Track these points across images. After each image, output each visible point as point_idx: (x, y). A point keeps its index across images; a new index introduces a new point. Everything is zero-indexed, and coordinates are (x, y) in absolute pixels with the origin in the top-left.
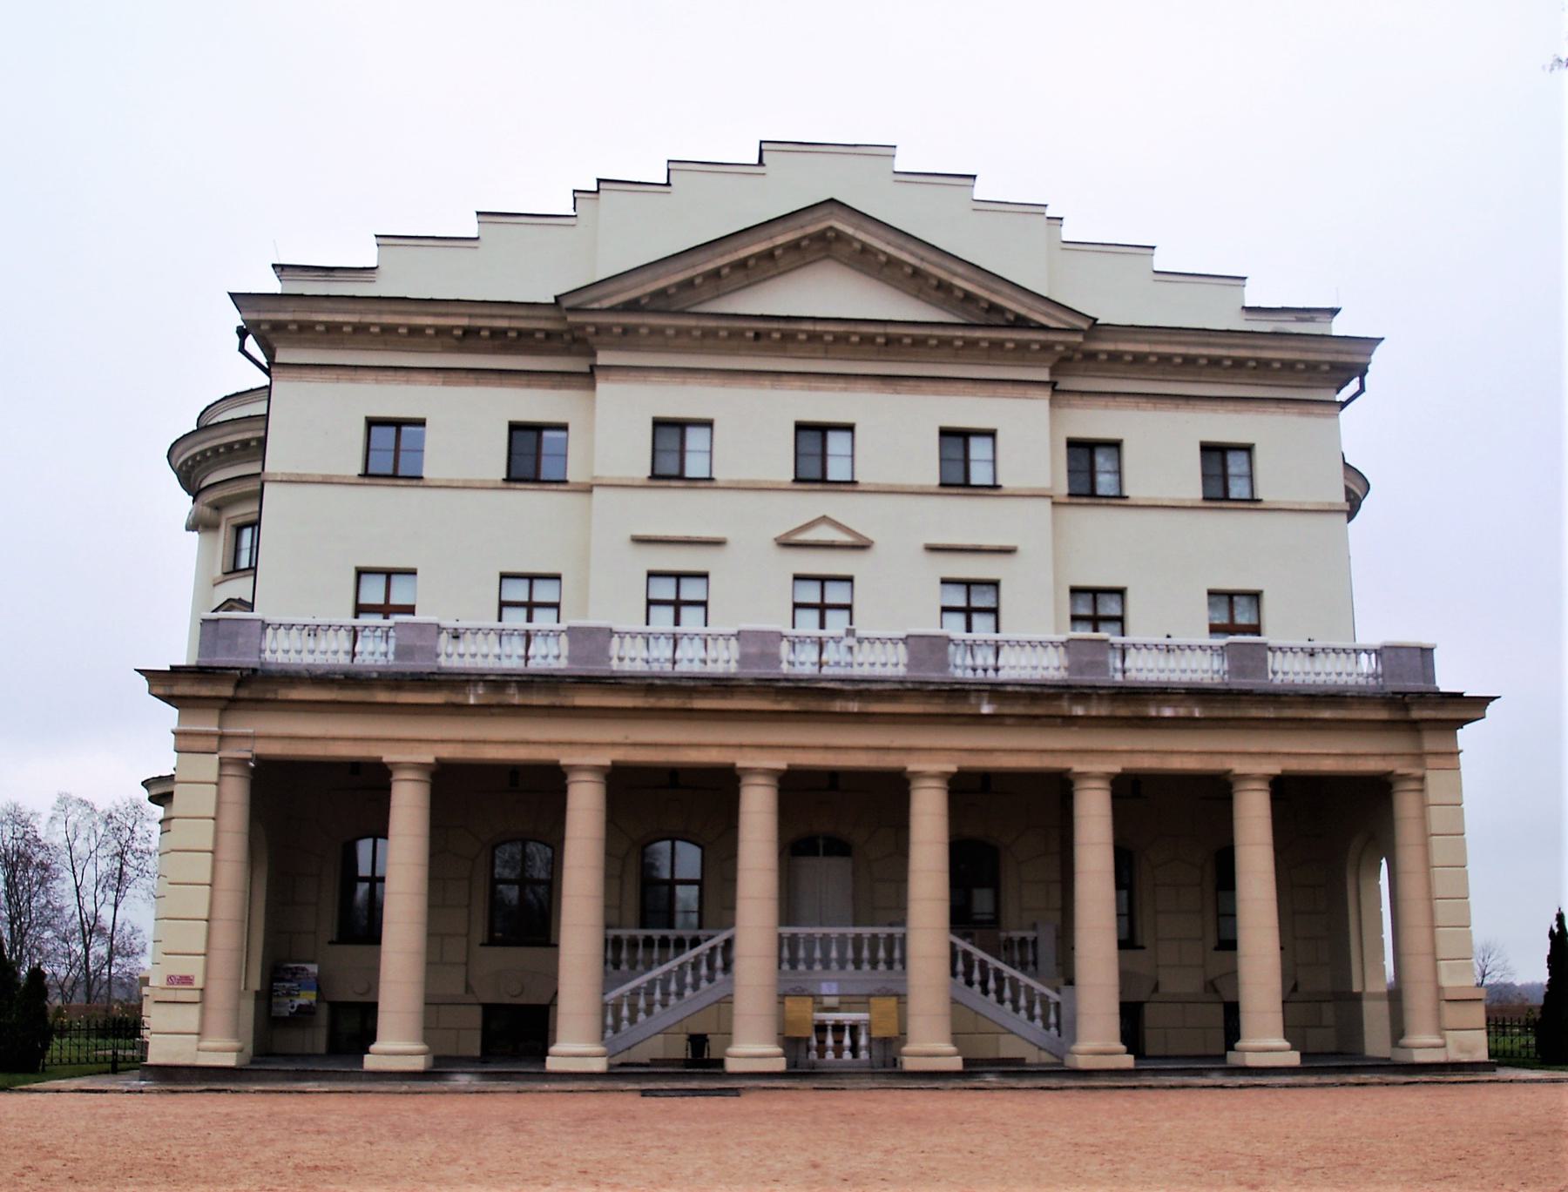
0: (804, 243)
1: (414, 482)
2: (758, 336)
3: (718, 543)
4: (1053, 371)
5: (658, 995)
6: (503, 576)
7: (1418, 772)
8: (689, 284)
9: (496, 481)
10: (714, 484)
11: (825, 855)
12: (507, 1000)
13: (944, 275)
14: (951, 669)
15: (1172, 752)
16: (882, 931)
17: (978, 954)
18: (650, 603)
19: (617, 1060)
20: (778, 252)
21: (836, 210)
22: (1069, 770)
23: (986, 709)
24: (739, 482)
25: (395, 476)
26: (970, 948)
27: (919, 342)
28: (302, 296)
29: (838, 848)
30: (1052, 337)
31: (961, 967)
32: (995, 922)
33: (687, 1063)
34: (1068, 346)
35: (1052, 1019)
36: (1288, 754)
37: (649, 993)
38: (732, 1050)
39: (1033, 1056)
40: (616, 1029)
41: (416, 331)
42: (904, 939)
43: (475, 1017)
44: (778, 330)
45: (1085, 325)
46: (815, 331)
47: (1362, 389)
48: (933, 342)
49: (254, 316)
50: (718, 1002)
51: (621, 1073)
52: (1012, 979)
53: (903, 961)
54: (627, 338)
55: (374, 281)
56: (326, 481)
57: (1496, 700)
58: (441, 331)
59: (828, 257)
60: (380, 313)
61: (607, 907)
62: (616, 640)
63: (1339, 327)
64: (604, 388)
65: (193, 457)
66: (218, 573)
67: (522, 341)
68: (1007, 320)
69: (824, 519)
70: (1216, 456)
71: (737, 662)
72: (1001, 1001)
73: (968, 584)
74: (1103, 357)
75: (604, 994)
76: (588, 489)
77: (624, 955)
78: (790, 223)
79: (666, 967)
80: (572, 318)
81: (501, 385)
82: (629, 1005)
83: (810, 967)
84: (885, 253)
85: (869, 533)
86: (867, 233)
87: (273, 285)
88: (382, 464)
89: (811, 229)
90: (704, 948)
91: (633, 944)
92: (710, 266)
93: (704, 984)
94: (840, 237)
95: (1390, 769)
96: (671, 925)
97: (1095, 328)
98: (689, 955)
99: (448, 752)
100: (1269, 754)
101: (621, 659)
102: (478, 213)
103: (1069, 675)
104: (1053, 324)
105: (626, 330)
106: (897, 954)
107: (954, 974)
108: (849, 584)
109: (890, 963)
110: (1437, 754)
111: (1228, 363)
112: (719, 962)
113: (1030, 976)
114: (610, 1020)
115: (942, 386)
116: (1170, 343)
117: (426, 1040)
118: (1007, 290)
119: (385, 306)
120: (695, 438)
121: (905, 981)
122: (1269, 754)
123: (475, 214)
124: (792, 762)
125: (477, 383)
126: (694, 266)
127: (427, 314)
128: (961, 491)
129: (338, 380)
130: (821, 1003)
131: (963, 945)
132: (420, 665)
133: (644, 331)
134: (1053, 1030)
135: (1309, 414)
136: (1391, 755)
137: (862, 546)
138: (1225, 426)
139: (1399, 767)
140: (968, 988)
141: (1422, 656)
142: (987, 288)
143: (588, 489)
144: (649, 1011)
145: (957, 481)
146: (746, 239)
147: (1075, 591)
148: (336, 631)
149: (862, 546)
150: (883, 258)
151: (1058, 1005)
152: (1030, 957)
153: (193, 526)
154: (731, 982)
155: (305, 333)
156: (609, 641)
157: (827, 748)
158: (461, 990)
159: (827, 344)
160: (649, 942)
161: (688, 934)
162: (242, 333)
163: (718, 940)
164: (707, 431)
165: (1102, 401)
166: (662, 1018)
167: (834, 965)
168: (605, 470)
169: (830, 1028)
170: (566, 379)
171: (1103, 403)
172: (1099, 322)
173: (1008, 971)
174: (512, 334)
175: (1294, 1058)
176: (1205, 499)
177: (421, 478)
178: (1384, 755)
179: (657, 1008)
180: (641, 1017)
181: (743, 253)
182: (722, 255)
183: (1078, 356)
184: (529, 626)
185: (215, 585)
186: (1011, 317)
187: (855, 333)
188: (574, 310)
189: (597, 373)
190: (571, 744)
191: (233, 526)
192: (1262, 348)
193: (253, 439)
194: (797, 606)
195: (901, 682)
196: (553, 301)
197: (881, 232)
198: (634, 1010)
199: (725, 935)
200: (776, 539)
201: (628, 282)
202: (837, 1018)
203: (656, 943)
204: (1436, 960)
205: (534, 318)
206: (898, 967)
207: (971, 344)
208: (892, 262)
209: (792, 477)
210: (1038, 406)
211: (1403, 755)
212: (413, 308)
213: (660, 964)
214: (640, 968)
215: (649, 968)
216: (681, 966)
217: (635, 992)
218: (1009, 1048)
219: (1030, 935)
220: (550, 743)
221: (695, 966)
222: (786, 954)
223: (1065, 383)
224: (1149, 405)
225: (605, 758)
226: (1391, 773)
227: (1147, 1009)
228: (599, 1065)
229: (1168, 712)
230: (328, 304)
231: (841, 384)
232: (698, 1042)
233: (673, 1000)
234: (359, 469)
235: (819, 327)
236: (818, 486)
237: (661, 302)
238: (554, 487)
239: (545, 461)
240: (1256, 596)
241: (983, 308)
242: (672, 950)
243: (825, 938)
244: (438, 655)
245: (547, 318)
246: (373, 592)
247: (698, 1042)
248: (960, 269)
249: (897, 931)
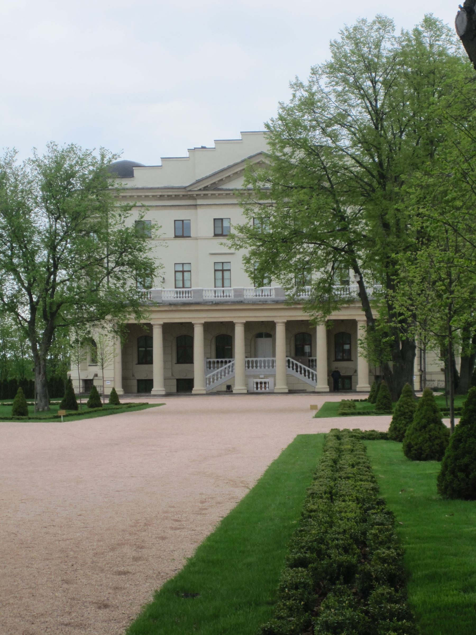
6: (175, 264)
8: (222, 180)
17: (299, 364)
33: (227, 392)
37: (217, 375)
40: (209, 384)
43: (175, 382)
54: (206, 196)
58: (153, 196)
61: (205, 353)
64: (200, 211)
67: (177, 197)
77: (212, 366)
80: (189, 193)
90: (231, 364)
91: (214, 362)
92: (227, 175)
94: (264, 163)
98: (228, 365)
114: (208, 382)
117: (164, 387)
131: (295, 362)
143: (196, 239)
144: (217, 379)
158: (171, 375)
160: (218, 362)
167: (263, 367)
173: (307, 368)
180: (215, 381)
181: (236, 171)
188: (190, 191)
190: (194, 318)
201: (204, 182)
213: (221, 367)
214: (216, 369)
215: (218, 368)
216: (226, 368)
217: (214, 375)
222: (247, 365)
225: (203, 321)
227: (353, 377)
228: (204, 392)
233: (223, 377)
237: (214, 187)
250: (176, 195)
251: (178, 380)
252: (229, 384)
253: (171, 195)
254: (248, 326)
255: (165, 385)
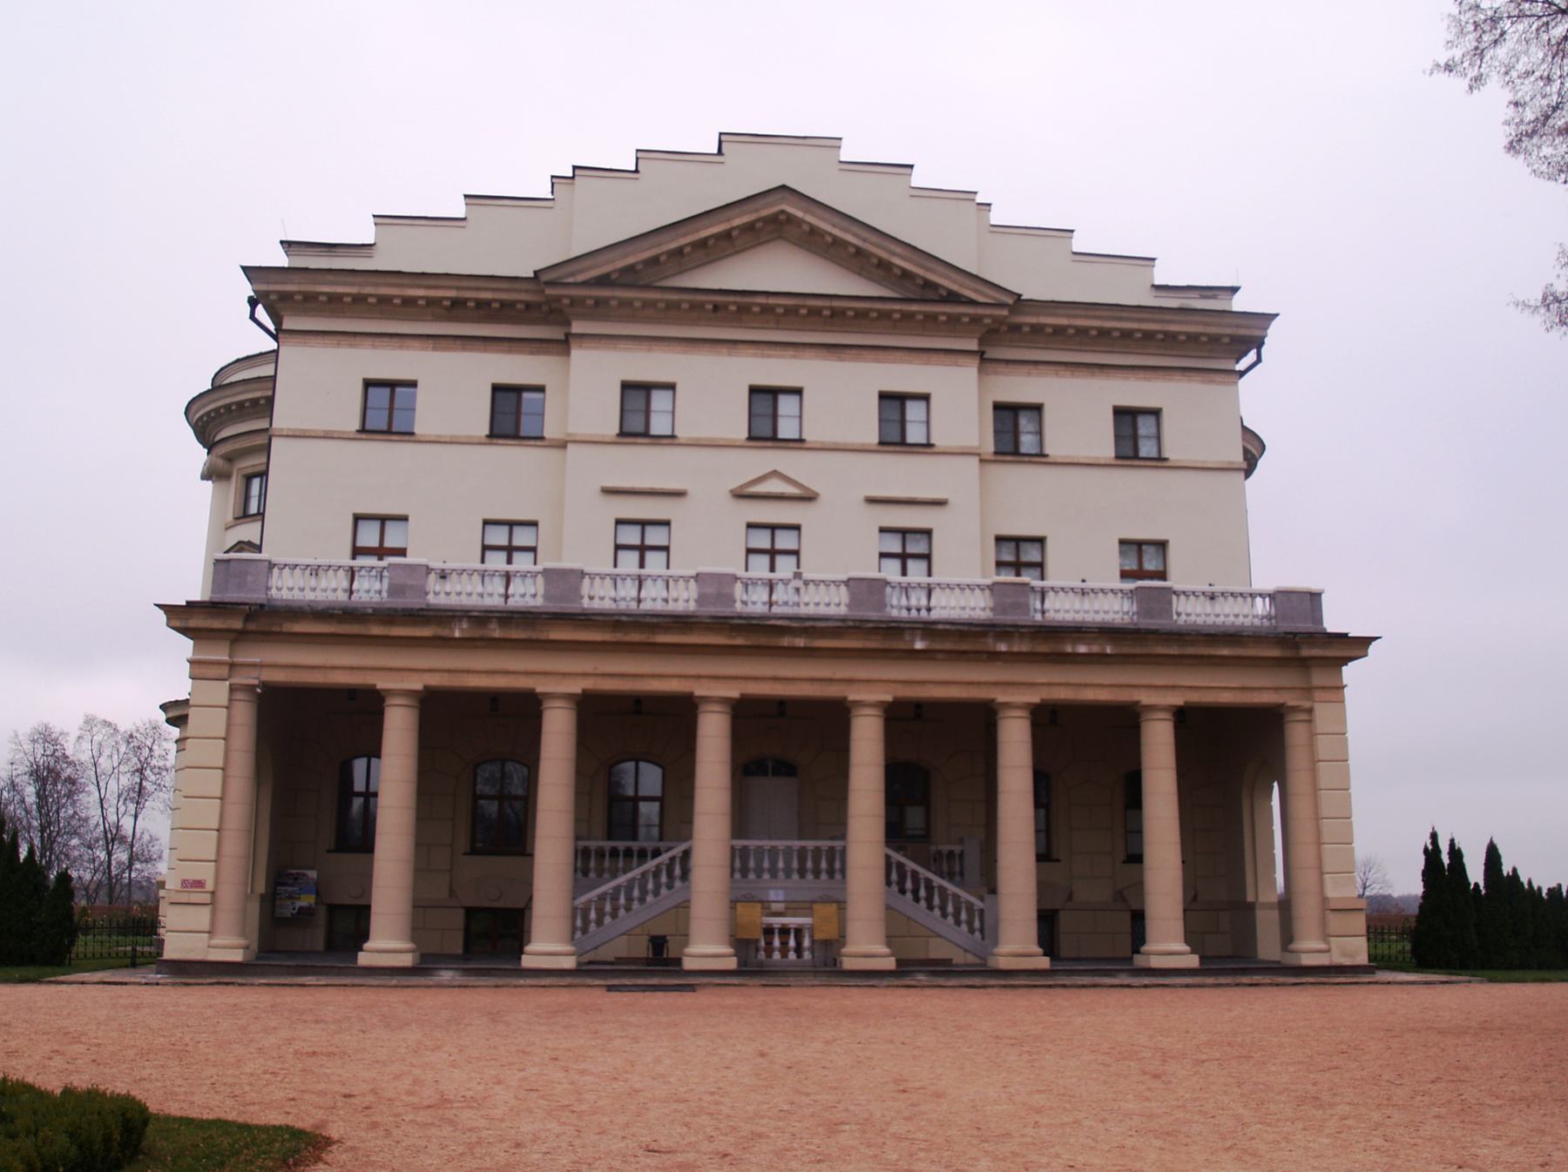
0: (759, 225)
1: (407, 438)
2: (716, 308)
3: (680, 494)
4: (981, 341)
5: (622, 901)
6: (486, 523)
7: (1306, 704)
8: (655, 261)
9: (480, 437)
10: (676, 441)
11: (773, 775)
12: (487, 904)
13: (884, 255)
14: (888, 609)
15: (1086, 685)
16: (824, 844)
17: (911, 865)
18: (618, 547)
19: (586, 958)
20: (735, 233)
21: (787, 195)
22: (993, 700)
23: (919, 645)
24: (698, 439)
25: (389, 432)
26: (903, 860)
27: (861, 315)
28: (306, 269)
29: (786, 769)
30: (980, 311)
31: (894, 876)
32: (926, 836)
33: (647, 961)
34: (994, 319)
35: (977, 924)
36: (1190, 687)
37: (615, 898)
38: (691, 950)
39: (959, 957)
40: (585, 930)
41: (409, 302)
42: (844, 851)
43: (458, 919)
44: (734, 303)
45: (1010, 301)
46: (767, 304)
47: (1259, 360)
48: (874, 315)
49: (263, 287)
50: (676, 907)
51: (590, 970)
52: (940, 887)
53: (843, 871)
54: (599, 309)
55: (372, 257)
56: (327, 436)
57: (1378, 640)
58: (431, 302)
59: (780, 237)
60: (377, 285)
61: (577, 821)
62: (587, 581)
63: (1239, 304)
64: (580, 356)
65: (208, 414)
66: (230, 518)
68: (941, 295)
69: (775, 474)
70: (1128, 419)
71: (696, 601)
72: (930, 907)
73: (904, 533)
74: (1026, 329)
75: (574, 899)
76: (562, 445)
77: (592, 864)
78: (746, 207)
79: (630, 875)
80: (549, 291)
81: (485, 351)
82: (596, 909)
83: (759, 876)
84: (831, 234)
85: (815, 487)
86: (815, 215)
87: (281, 260)
88: (378, 420)
89: (765, 213)
90: (664, 858)
91: (601, 854)
92: (674, 245)
93: (664, 891)
94: (791, 219)
95: (1282, 701)
96: (635, 837)
97: (1019, 303)
98: (651, 864)
99: (435, 680)
100: (1174, 687)
101: (591, 598)
102: (466, 196)
103: (994, 615)
104: (981, 299)
105: (598, 302)
106: (837, 865)
107: (888, 883)
108: (796, 532)
109: (831, 873)
110: (1323, 688)
111: (1139, 335)
112: (677, 871)
113: (957, 885)
114: (579, 923)
115: (881, 355)
116: (1087, 317)
117: (413, 939)
118: (940, 268)
119: (382, 280)
120: (659, 400)
121: (844, 889)
122: (1174, 687)
123: (463, 197)
124: (744, 692)
125: (464, 349)
126: (659, 245)
127: (420, 287)
128: (898, 449)
129: (339, 345)
130: (769, 908)
131: (897, 857)
132: (410, 601)
133: (614, 303)
134: (977, 934)
135: (1211, 382)
136: (1283, 688)
137: (809, 497)
138: (1136, 392)
139: (1290, 699)
140: (900, 895)
141: (1311, 600)
142: (922, 267)
143: (562, 445)
144: (614, 915)
145: (894, 440)
146: (706, 221)
147: (1000, 540)
148: (336, 571)
149: (809, 497)
150: (829, 239)
151: (982, 911)
152: (957, 869)
153: (207, 476)
154: (688, 889)
155: (310, 303)
156: (581, 582)
157: (776, 679)
159: (779, 315)
160: (614, 853)
161: (649, 846)
162: (253, 303)
163: (678, 850)
164: (669, 393)
165: (1025, 369)
166: (627, 921)
167: (781, 875)
168: (577, 428)
169: (776, 931)
170: (544, 345)
171: (1027, 371)
172: (1023, 298)
174: (495, 305)
175: (1193, 961)
176: (1117, 457)
177: (412, 434)
178: (1276, 689)
179: (622, 912)
180: (607, 920)
182: (685, 236)
183: (1004, 328)
184: (510, 568)
185: (227, 529)
186: (944, 293)
187: (804, 306)
189: (572, 341)
190: (546, 674)
191: (244, 476)
192: (1168, 322)
193: (262, 398)
194: (750, 551)
195: (843, 620)
196: (532, 275)
197: (828, 215)
198: (601, 913)
199: (683, 847)
200: (731, 491)
202: (784, 922)
203: (621, 854)
204: (1322, 874)
205: (515, 290)
206: (838, 876)
207: (908, 317)
208: (838, 242)
209: (745, 435)
210: (968, 373)
211: (1293, 689)
212: (406, 281)
213: (625, 872)
214: (606, 876)
215: (615, 876)
216: (644, 874)
217: (602, 897)
218: (938, 950)
219: (957, 848)
220: (527, 673)
221: (656, 874)
222: (738, 864)
223: (992, 353)
224: (1069, 373)
225: (576, 687)
226: (1282, 705)
227: (1063, 916)
228: (569, 963)
229: (1082, 649)
230: (331, 277)
231: (791, 352)
232: (658, 943)
233: (636, 905)
234: (357, 425)
235: (772, 301)
236: (769, 444)
237: (629, 276)
238: (532, 442)
239: (524, 420)
240: (1162, 545)
241: (918, 285)
242: (635, 859)
243: (774, 850)
244: (427, 593)
245: (527, 291)
246: (369, 537)
247: (658, 943)
248: (898, 250)
249: (838, 844)
250: (503, 304)
251: (471, 912)
252: (658, 932)
253: (488, 303)
254: (746, 713)
255: (418, 929)
